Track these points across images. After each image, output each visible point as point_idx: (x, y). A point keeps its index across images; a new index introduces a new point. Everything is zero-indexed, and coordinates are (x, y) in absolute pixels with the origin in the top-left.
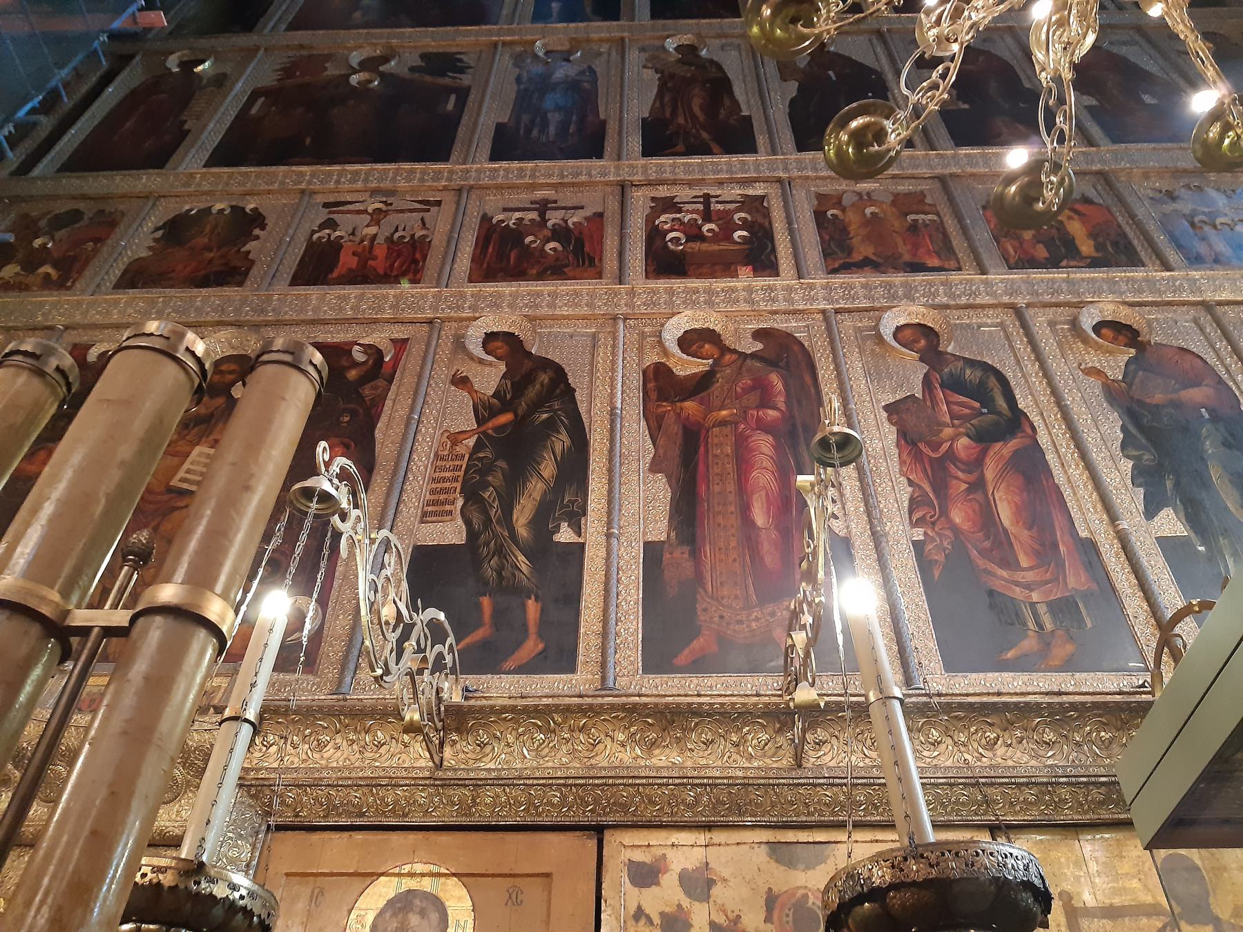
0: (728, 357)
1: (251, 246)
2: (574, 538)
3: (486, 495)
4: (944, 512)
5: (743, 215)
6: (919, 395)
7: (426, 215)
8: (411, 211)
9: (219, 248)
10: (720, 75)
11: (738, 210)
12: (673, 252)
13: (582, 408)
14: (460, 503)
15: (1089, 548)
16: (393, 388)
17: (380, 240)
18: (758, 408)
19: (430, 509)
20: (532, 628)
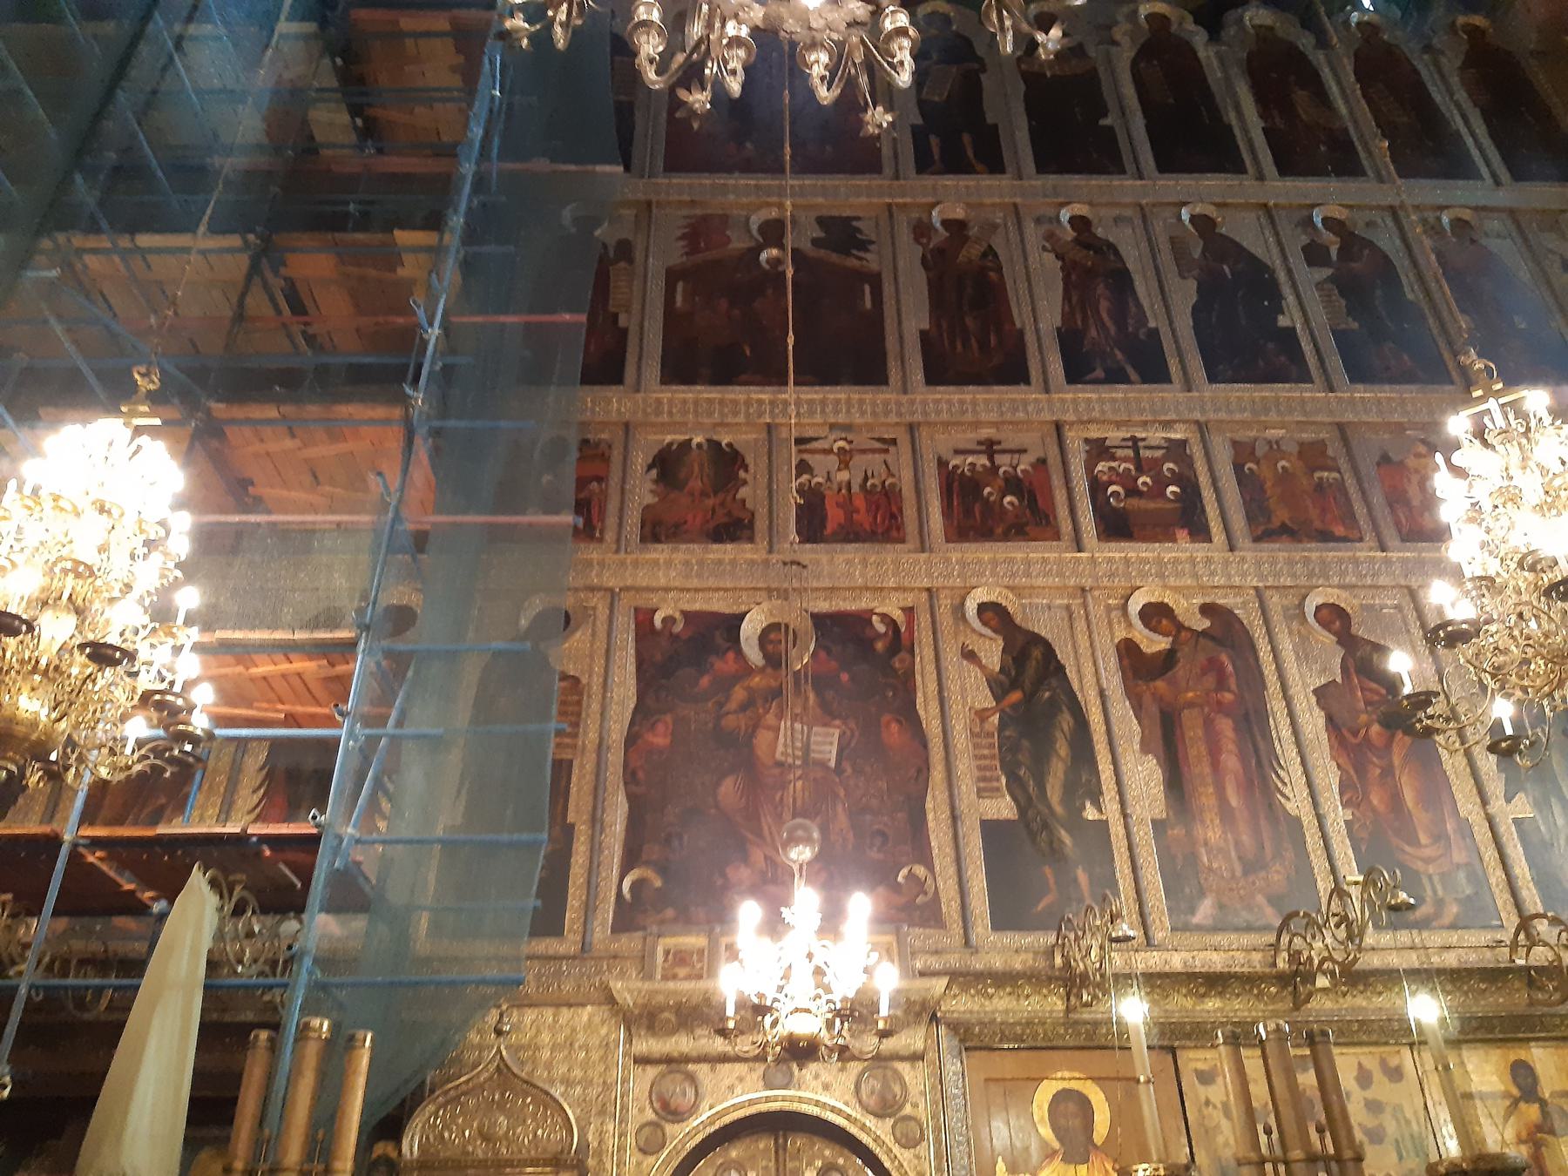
1: (743, 492)
3: (1022, 773)
4: (1366, 795)
5: (1171, 465)
6: (1339, 680)
8: (874, 451)
9: (715, 493)
10: (1119, 265)
11: (1165, 459)
12: (1114, 509)
13: (1076, 686)
14: (1004, 780)
15: (1465, 828)
16: (918, 659)
17: (855, 488)
19: (982, 785)
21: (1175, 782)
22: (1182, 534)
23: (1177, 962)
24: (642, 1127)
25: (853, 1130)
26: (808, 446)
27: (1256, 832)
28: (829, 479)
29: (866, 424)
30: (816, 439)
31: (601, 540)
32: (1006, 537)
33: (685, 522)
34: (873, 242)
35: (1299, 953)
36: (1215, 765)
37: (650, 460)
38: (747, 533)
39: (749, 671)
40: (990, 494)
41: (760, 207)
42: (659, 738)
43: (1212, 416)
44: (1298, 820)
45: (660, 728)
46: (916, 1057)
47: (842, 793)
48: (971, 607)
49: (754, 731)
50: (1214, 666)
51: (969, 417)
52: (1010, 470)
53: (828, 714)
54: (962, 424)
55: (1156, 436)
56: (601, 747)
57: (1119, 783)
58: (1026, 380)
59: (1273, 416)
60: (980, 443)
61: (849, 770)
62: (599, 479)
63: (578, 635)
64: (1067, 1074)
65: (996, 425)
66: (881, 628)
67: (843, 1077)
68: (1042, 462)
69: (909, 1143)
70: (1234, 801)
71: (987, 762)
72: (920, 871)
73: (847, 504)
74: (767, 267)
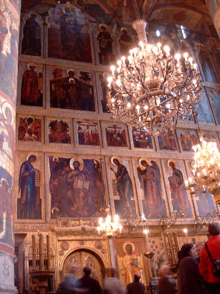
1: (68, 133)
6: (172, 176)
8: (93, 126)
9: (63, 132)
13: (130, 176)
14: (118, 193)
20: (131, 213)
22: (148, 147)
24: (59, 252)
26: (80, 124)
30: (82, 122)
32: (118, 146)
33: (57, 138)
34: (91, 79)
35: (165, 222)
36: (152, 190)
37: (49, 124)
38: (69, 142)
39: (71, 170)
40: (115, 137)
41: (70, 68)
44: (164, 200)
47: (90, 195)
53: (87, 179)
57: (137, 193)
61: (91, 190)
64: (128, 242)
65: (116, 122)
66: (95, 163)
68: (124, 131)
69: (103, 253)
70: (155, 197)
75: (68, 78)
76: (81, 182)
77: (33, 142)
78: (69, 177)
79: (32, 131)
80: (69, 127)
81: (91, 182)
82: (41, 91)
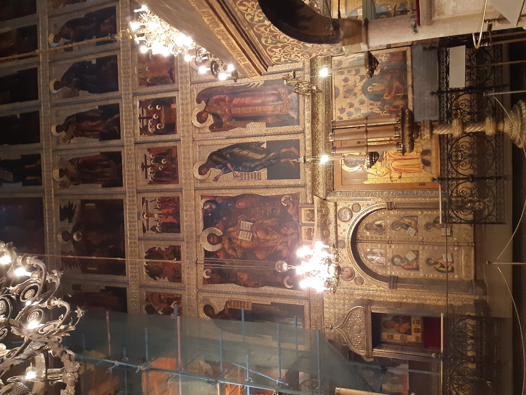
0: (207, 110)
1: (163, 249)
2: (266, 143)
3: (253, 166)
5: (149, 107)
7: (149, 201)
8: (147, 205)
11: (147, 109)
12: (165, 127)
14: (256, 171)
16: (218, 195)
17: (160, 212)
18: (225, 102)
19: (257, 178)
20: (289, 150)
21: (256, 118)
22: (173, 106)
23: (308, 125)
24: (356, 283)
25: (356, 223)
26: (146, 227)
27: (269, 95)
28: (158, 221)
29: (137, 207)
31: (181, 295)
32: (177, 164)
33: (174, 268)
34: (69, 202)
39: (223, 249)
42: (245, 277)
43: (131, 91)
44: (265, 81)
45: (241, 276)
46: (336, 205)
47: (260, 221)
48: (200, 177)
49: (242, 247)
50: (218, 101)
51: (134, 173)
52: (152, 161)
53: (236, 224)
54: (136, 175)
55: (138, 111)
56: (248, 294)
58: (120, 152)
59: (130, 70)
60: (143, 170)
62: (160, 296)
63: (213, 302)
65: (136, 164)
66: (208, 206)
67: (341, 225)
71: (250, 176)
72: (282, 200)
73: (166, 215)
74: (80, 239)
75: (74, 241)
76: (240, 234)
77: (183, 308)
78: (234, 254)
79: (166, 308)
80: (155, 246)
81: (240, 217)
82: (101, 288)
